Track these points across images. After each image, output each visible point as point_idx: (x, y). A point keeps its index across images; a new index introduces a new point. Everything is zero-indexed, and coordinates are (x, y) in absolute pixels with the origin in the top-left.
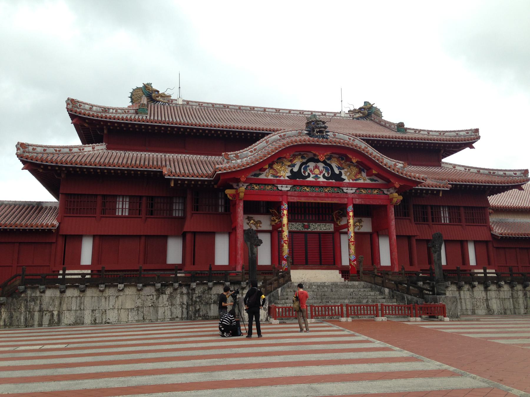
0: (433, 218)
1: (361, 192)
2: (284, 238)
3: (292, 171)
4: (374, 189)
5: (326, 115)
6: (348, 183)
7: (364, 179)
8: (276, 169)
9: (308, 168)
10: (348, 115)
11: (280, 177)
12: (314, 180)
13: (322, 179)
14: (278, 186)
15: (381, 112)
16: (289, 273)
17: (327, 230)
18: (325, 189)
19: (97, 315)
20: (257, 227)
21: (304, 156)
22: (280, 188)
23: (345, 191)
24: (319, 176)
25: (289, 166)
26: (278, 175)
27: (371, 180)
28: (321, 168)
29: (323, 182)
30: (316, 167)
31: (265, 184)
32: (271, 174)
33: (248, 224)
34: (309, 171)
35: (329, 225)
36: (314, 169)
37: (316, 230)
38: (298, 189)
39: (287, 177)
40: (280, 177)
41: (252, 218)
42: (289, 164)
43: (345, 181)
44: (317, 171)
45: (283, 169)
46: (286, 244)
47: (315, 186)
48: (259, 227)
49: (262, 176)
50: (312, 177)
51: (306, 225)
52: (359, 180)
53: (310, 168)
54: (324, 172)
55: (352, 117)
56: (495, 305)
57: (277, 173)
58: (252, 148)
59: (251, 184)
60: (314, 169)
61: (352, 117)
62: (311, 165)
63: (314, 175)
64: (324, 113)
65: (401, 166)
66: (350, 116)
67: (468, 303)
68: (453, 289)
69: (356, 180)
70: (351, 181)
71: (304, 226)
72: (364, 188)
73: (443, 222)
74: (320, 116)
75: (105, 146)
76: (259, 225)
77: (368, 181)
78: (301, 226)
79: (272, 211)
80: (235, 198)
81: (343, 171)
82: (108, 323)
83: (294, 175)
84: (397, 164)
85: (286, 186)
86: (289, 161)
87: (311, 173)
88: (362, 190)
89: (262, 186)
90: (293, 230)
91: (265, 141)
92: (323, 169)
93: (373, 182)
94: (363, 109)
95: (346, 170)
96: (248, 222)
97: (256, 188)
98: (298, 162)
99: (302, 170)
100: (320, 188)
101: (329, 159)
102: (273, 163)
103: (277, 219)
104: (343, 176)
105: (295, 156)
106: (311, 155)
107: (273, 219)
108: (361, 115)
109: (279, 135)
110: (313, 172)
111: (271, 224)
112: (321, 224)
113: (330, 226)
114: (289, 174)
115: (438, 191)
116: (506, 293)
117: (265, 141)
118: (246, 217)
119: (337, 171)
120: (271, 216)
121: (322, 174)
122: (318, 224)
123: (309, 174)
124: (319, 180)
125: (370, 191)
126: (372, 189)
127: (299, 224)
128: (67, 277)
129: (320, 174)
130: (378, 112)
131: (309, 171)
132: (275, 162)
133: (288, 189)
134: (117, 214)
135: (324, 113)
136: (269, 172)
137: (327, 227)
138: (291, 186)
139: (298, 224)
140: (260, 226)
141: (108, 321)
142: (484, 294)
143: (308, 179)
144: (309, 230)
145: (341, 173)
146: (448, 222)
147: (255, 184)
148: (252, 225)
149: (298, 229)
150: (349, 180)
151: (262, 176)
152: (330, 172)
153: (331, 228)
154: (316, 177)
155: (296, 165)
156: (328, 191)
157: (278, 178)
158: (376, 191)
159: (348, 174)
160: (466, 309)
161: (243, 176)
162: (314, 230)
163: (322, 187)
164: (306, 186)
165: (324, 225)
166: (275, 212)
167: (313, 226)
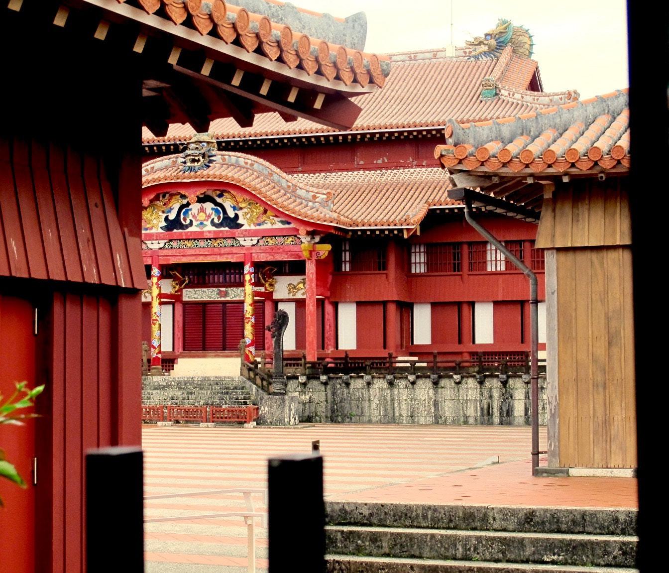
0: (470, 264)
1: (267, 242)
3: (166, 219)
4: (287, 236)
5: (417, 58)
6: (246, 230)
7: (273, 224)
9: (190, 212)
10: (461, 53)
11: (151, 228)
12: (198, 229)
13: (209, 228)
15: (530, 37)
18: (214, 241)
22: (150, 246)
23: (242, 243)
24: (205, 223)
25: (163, 212)
26: (148, 226)
27: (283, 222)
28: (209, 211)
29: (210, 232)
30: (202, 210)
34: (191, 217)
37: (237, 298)
38: (175, 244)
39: (161, 228)
43: (243, 228)
44: (202, 216)
45: (153, 217)
51: (223, 291)
52: (265, 225)
53: (192, 212)
54: (213, 216)
55: (468, 54)
56: (448, 410)
61: (468, 54)
62: (195, 207)
63: (199, 222)
64: (412, 56)
65: (323, 199)
66: (465, 53)
67: (404, 406)
68: (381, 386)
69: (259, 225)
70: (253, 227)
71: (220, 293)
72: (273, 236)
73: (489, 269)
74: (404, 61)
77: (279, 225)
81: (240, 213)
83: (172, 225)
84: (318, 195)
87: (193, 220)
88: (268, 240)
90: (205, 299)
92: (211, 211)
93: (287, 226)
94: (489, 37)
95: (245, 210)
98: (176, 207)
99: (182, 216)
100: (207, 241)
101: (220, 196)
103: (177, 284)
104: (240, 221)
108: (486, 48)
110: (198, 218)
115: (401, 231)
116: (470, 391)
119: (231, 214)
121: (210, 220)
123: (191, 221)
124: (205, 229)
125: (280, 240)
126: (284, 236)
127: (213, 290)
129: (207, 220)
130: (521, 38)
133: (162, 245)
135: (412, 56)
138: (166, 241)
139: (211, 289)
142: (431, 392)
143: (190, 229)
144: (228, 299)
145: (237, 216)
146: (503, 269)
149: (211, 297)
150: (250, 225)
152: (222, 215)
158: (290, 239)
159: (249, 215)
160: (400, 415)
162: (235, 299)
163: (210, 239)
164: (186, 239)
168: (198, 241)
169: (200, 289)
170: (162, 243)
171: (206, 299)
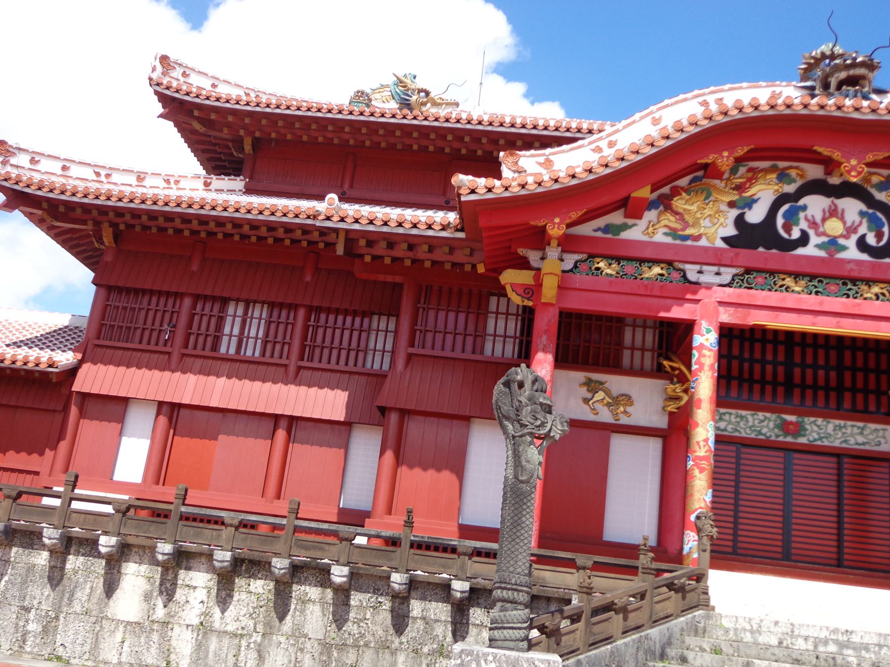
2: (697, 448)
3: (740, 221)
8: (681, 211)
9: (802, 215)
11: (698, 238)
12: (822, 254)
13: (852, 253)
14: (688, 267)
16: (700, 578)
17: (867, 447)
18: (865, 288)
19: (32, 627)
20: (615, 415)
21: (788, 175)
22: (692, 276)
24: (842, 241)
25: (732, 205)
26: (689, 231)
30: (833, 213)
31: (642, 261)
32: (666, 226)
33: (586, 401)
34: (804, 225)
35: (876, 430)
36: (824, 220)
37: (826, 443)
39: (725, 239)
40: (698, 238)
41: (602, 383)
42: (734, 197)
44: (834, 227)
45: (707, 212)
46: (702, 470)
47: (826, 277)
48: (621, 416)
49: (636, 233)
50: (817, 246)
51: (791, 423)
53: (809, 212)
57: (686, 225)
58: (600, 139)
59: (592, 256)
60: (824, 220)
62: (815, 204)
63: (825, 239)
71: (785, 427)
75: (243, 183)
76: (622, 409)
78: (771, 425)
79: (671, 367)
80: (529, 299)
82: (59, 658)
85: (715, 269)
86: (733, 189)
87: (811, 233)
89: (630, 267)
90: (744, 435)
91: (649, 119)
92: (857, 219)
96: (589, 395)
97: (609, 271)
99: (780, 221)
102: (676, 192)
105: (754, 176)
106: (814, 171)
107: (674, 391)
109: (701, 99)
110: (821, 229)
111: (664, 408)
112: (849, 423)
113: (881, 433)
114: (731, 231)
117: (649, 119)
118: (583, 380)
120: (669, 382)
121: (854, 238)
122: (837, 422)
127: (766, 418)
128: (75, 505)
129: (846, 237)
131: (804, 225)
132: (682, 188)
134: (223, 350)
136: (659, 222)
137: (871, 437)
139: (761, 415)
140: (625, 412)
141: (60, 651)
143: (800, 251)
144: (802, 440)
147: (605, 257)
148: (597, 405)
149: (760, 433)
151: (636, 233)
153: (883, 441)
154: (832, 244)
155: (755, 201)
156: (876, 295)
157: (689, 243)
161: (557, 220)
162: (819, 443)
163: (854, 281)
164: (790, 274)
165: (859, 428)
166: (679, 369)
167: (815, 428)
168: (820, 281)
169: (733, 411)
170: (728, 274)
171: (745, 433)
